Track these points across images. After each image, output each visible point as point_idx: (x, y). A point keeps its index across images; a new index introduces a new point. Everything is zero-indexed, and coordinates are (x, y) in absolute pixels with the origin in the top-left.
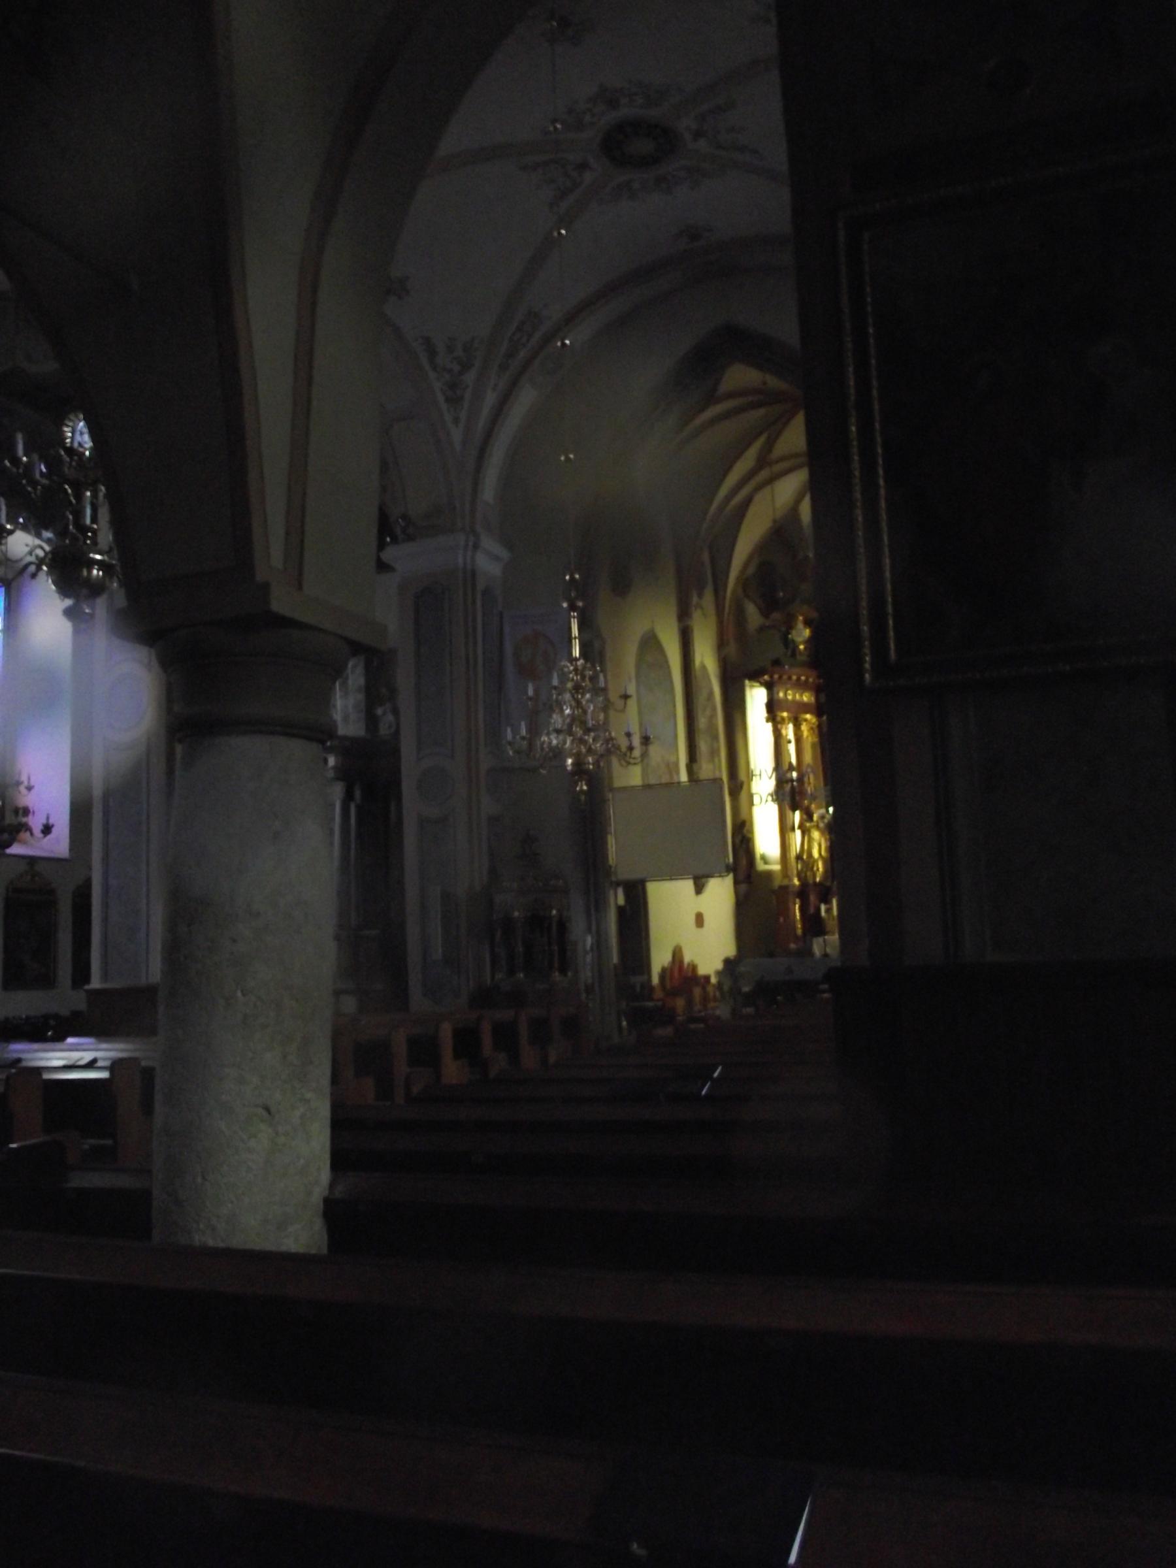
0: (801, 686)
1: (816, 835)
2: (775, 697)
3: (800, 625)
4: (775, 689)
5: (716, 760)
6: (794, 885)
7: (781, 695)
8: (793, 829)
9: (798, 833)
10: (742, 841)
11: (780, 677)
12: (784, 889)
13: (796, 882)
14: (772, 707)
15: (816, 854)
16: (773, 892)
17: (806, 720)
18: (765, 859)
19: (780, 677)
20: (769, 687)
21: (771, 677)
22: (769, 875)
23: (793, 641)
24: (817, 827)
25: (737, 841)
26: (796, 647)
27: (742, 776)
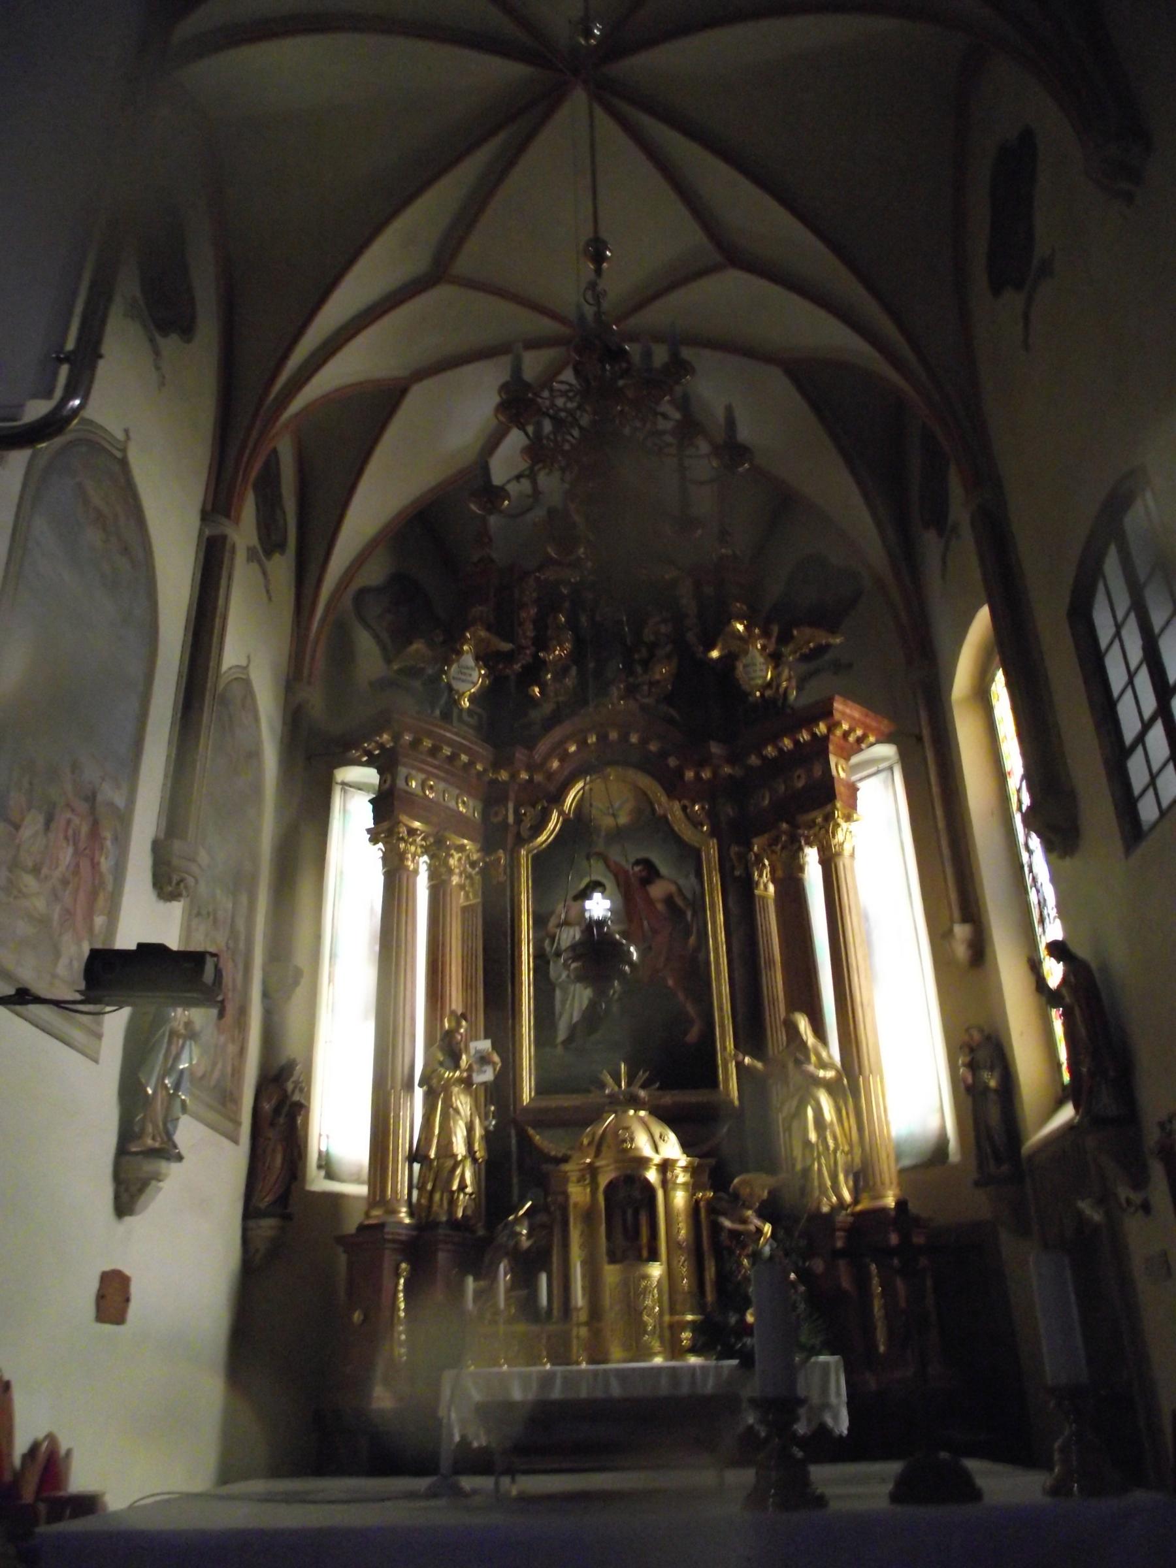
0: (455, 772)
1: (463, 1103)
2: (401, 783)
3: (468, 660)
4: (403, 771)
5: (244, 899)
6: (400, 1223)
8: (409, 1087)
9: (419, 1093)
10: (277, 1111)
11: (416, 743)
12: (372, 1233)
13: (404, 1216)
14: (386, 806)
15: (460, 1148)
16: (342, 1240)
17: (461, 848)
18: (327, 1166)
19: (416, 743)
20: (385, 763)
21: (396, 737)
22: (335, 1200)
23: (450, 688)
24: (467, 1083)
25: (267, 1107)
26: (456, 703)
27: (301, 959)
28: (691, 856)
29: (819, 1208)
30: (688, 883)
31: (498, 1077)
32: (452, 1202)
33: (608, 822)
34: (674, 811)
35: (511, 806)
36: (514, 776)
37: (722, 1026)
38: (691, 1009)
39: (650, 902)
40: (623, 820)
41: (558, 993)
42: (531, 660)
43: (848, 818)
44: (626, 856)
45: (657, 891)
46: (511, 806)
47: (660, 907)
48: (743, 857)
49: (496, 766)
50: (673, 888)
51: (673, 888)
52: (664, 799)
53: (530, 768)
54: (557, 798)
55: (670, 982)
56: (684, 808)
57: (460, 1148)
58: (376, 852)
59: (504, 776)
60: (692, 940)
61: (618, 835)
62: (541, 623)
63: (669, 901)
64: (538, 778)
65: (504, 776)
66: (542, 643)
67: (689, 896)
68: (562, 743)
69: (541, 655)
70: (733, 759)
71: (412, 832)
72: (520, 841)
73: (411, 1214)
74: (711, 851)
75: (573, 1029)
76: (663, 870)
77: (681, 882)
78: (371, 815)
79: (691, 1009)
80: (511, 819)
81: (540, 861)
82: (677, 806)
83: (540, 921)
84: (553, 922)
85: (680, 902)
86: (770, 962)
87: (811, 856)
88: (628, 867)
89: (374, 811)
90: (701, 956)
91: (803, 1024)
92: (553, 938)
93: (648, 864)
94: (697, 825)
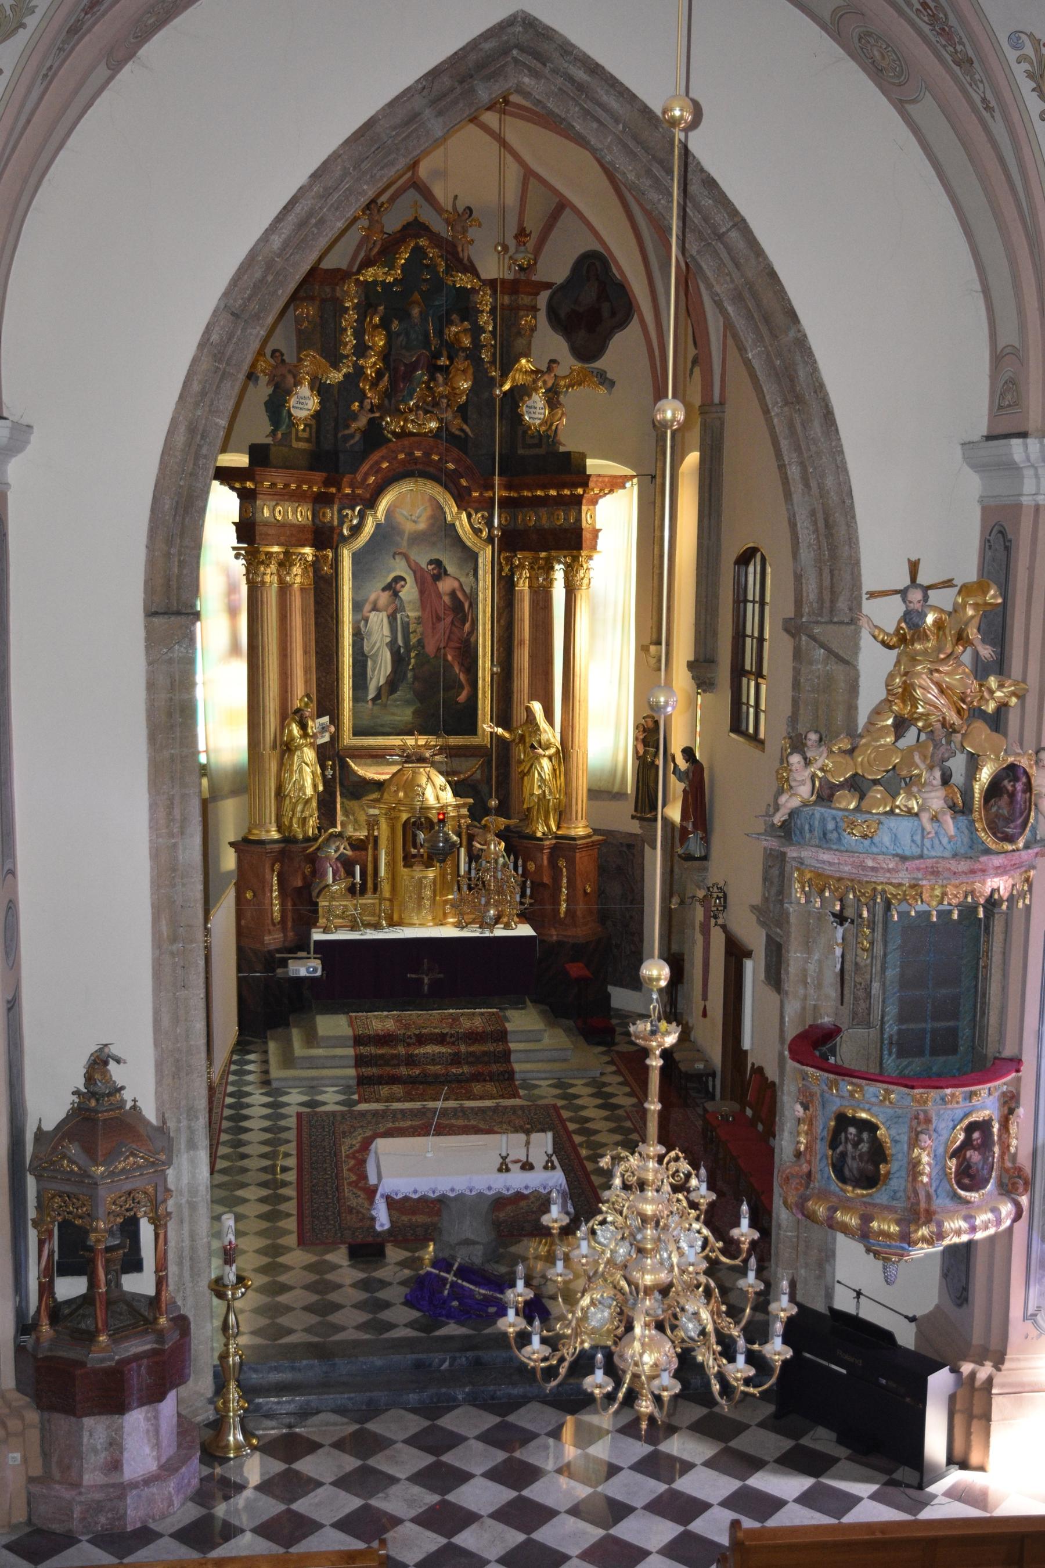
0: (297, 497)
3: (304, 390)
7: (266, 513)
13: (275, 835)
14: (247, 530)
23: (290, 415)
28: (471, 557)
29: (535, 832)
30: (467, 581)
31: (332, 737)
32: (304, 821)
33: (409, 527)
34: (463, 524)
35: (336, 508)
36: (339, 490)
37: (484, 692)
38: (462, 677)
39: (439, 596)
40: (422, 526)
41: (370, 663)
42: (351, 370)
43: (590, 558)
44: (423, 558)
45: (445, 586)
46: (336, 508)
47: (446, 599)
48: (510, 561)
49: (327, 483)
50: (456, 584)
51: (456, 584)
52: (455, 509)
53: (352, 486)
54: (371, 504)
55: (450, 658)
56: (469, 516)
57: (309, 791)
58: (239, 567)
59: (333, 490)
60: (467, 625)
61: (417, 539)
62: (359, 334)
63: (453, 594)
64: (359, 491)
65: (333, 490)
66: (362, 349)
67: (468, 590)
68: (378, 463)
69: (361, 362)
70: (508, 487)
71: (269, 555)
72: (345, 540)
73: (279, 831)
74: (486, 556)
75: (379, 689)
76: (450, 570)
77: (462, 580)
78: (235, 535)
79: (462, 677)
80: (336, 523)
81: (356, 557)
82: (464, 516)
83: (357, 606)
84: (367, 607)
85: (460, 595)
86: (522, 642)
87: (559, 574)
88: (424, 566)
89: (237, 531)
90: (473, 639)
91: (537, 707)
92: (366, 620)
93: (438, 563)
94: (477, 532)
